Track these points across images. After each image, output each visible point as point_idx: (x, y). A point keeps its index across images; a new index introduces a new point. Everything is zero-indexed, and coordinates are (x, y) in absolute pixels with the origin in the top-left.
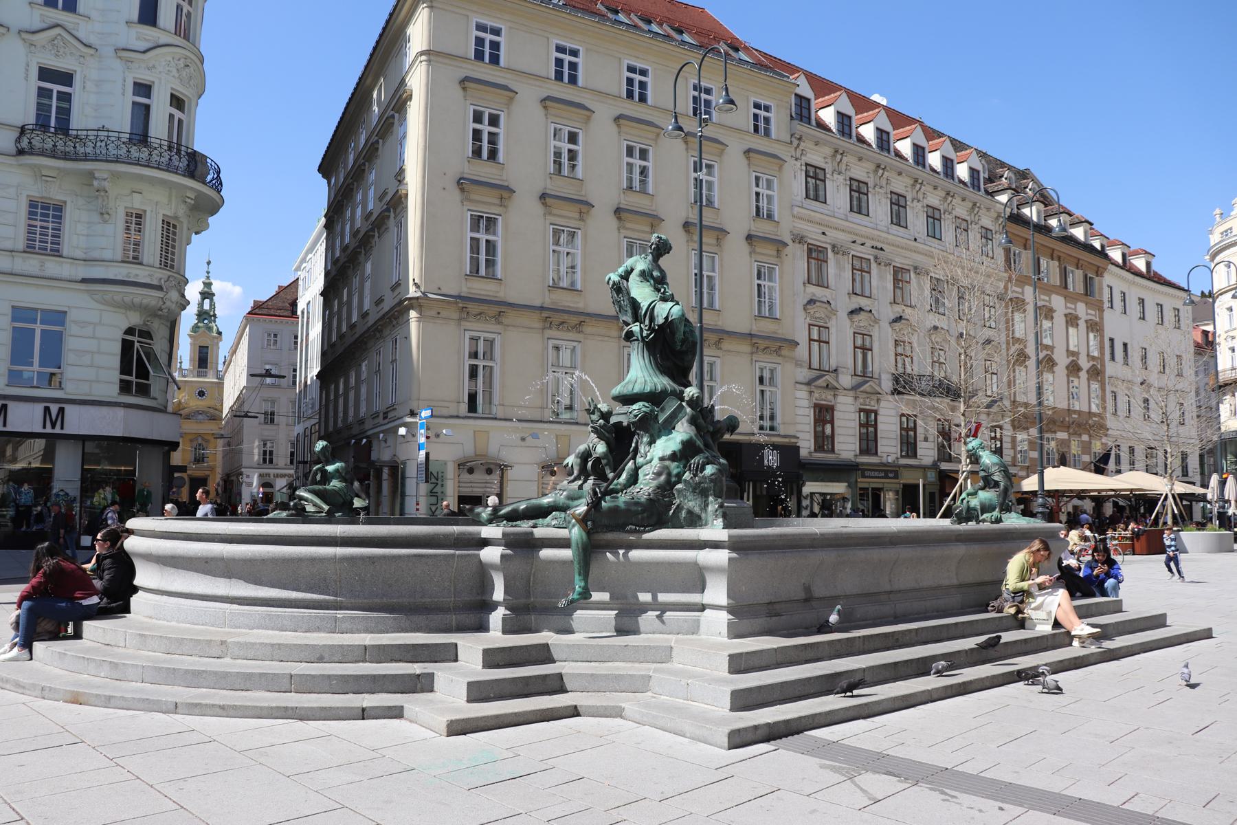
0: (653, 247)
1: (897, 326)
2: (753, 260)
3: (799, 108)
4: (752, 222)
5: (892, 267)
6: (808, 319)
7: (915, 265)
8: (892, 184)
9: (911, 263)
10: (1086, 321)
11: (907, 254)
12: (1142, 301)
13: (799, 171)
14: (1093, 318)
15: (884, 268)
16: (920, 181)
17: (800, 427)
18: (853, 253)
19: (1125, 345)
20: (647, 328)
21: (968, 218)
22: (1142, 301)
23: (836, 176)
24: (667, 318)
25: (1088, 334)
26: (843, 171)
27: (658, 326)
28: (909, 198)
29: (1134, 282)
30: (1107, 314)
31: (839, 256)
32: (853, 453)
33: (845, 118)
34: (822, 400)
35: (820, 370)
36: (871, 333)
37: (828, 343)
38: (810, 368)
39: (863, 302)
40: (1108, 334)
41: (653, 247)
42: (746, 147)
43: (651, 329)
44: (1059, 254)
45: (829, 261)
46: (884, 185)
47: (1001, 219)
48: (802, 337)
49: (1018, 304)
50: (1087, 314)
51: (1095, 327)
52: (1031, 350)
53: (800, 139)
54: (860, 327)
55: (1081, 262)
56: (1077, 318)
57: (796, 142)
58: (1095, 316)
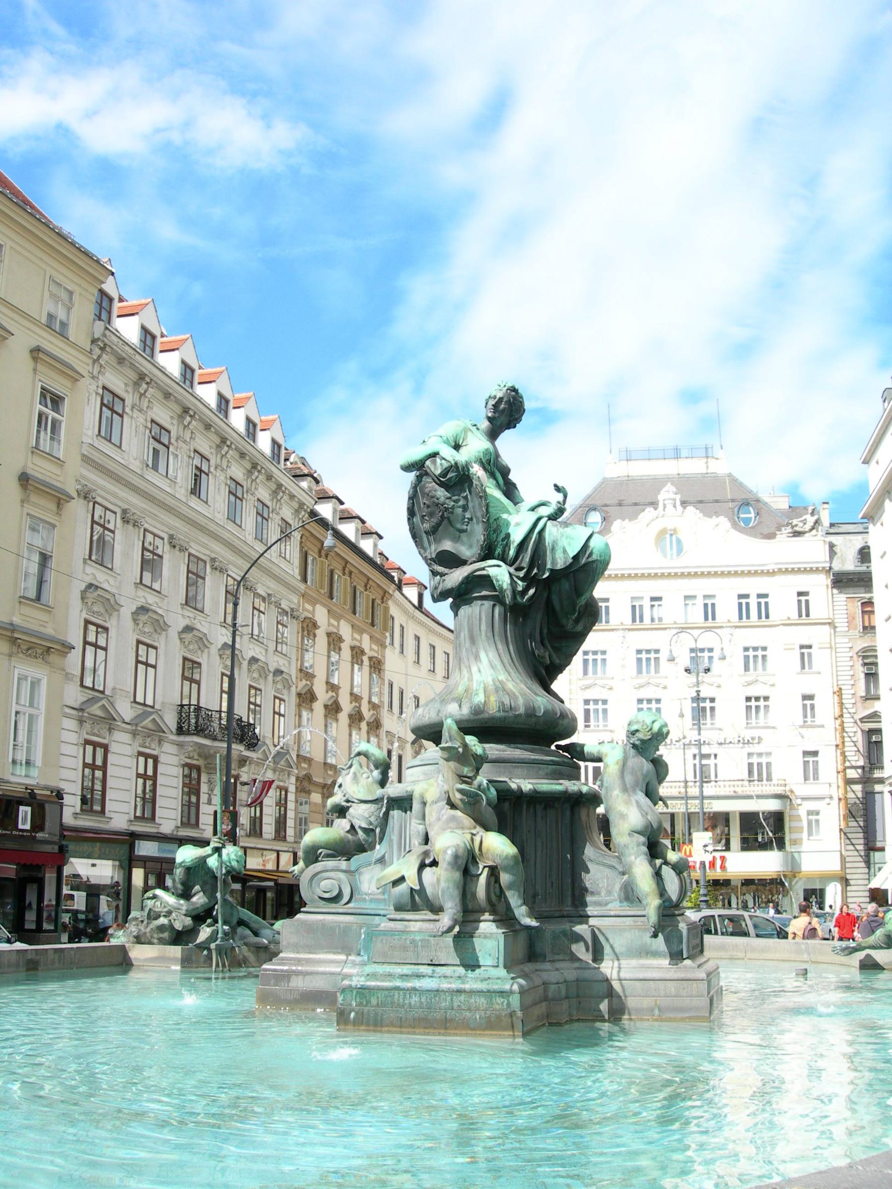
0: (502, 406)
1: (188, 636)
2: (25, 513)
3: (98, 307)
4: (30, 453)
5: (187, 554)
6: (84, 612)
7: (213, 556)
8: (196, 439)
9: (208, 552)
10: (370, 658)
11: (205, 539)
12: (417, 638)
13: (94, 394)
14: (376, 655)
15: (178, 553)
16: (228, 443)
17: (66, 774)
18: (146, 526)
19: (402, 693)
20: (521, 574)
21: (269, 503)
22: (417, 638)
23: (136, 414)
24: (576, 558)
25: (370, 674)
26: (145, 409)
27: (552, 571)
28: (213, 462)
29: (414, 616)
30: (388, 652)
31: (130, 527)
32: (126, 817)
33: (148, 336)
34: (94, 735)
35: (93, 689)
36: (156, 644)
37: (105, 649)
38: (82, 685)
39: (151, 599)
40: (388, 676)
41: (502, 406)
42: (34, 344)
43: (530, 580)
44: (353, 569)
45: (117, 532)
46: (188, 440)
47: (303, 513)
48: (75, 637)
49: (309, 627)
50: (371, 649)
51: (377, 666)
52: (319, 688)
53: (102, 349)
54: (145, 633)
55: (370, 582)
56: (363, 652)
57: (97, 351)
58: (377, 652)
